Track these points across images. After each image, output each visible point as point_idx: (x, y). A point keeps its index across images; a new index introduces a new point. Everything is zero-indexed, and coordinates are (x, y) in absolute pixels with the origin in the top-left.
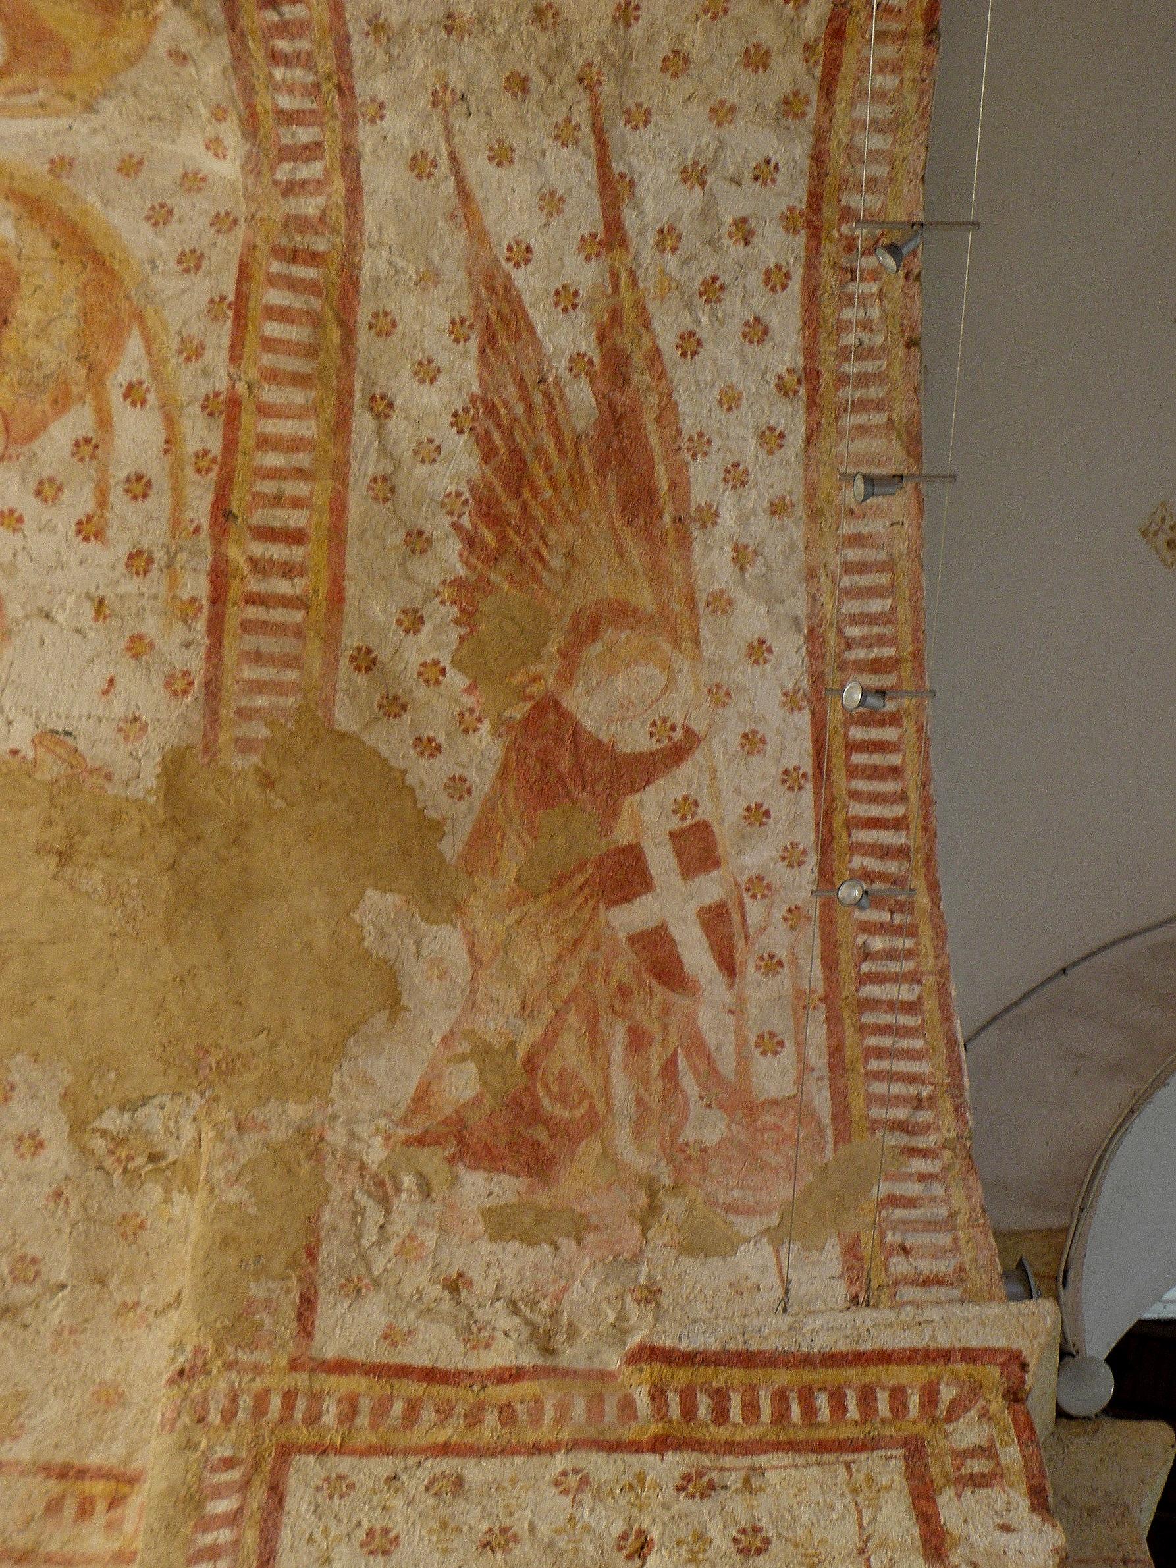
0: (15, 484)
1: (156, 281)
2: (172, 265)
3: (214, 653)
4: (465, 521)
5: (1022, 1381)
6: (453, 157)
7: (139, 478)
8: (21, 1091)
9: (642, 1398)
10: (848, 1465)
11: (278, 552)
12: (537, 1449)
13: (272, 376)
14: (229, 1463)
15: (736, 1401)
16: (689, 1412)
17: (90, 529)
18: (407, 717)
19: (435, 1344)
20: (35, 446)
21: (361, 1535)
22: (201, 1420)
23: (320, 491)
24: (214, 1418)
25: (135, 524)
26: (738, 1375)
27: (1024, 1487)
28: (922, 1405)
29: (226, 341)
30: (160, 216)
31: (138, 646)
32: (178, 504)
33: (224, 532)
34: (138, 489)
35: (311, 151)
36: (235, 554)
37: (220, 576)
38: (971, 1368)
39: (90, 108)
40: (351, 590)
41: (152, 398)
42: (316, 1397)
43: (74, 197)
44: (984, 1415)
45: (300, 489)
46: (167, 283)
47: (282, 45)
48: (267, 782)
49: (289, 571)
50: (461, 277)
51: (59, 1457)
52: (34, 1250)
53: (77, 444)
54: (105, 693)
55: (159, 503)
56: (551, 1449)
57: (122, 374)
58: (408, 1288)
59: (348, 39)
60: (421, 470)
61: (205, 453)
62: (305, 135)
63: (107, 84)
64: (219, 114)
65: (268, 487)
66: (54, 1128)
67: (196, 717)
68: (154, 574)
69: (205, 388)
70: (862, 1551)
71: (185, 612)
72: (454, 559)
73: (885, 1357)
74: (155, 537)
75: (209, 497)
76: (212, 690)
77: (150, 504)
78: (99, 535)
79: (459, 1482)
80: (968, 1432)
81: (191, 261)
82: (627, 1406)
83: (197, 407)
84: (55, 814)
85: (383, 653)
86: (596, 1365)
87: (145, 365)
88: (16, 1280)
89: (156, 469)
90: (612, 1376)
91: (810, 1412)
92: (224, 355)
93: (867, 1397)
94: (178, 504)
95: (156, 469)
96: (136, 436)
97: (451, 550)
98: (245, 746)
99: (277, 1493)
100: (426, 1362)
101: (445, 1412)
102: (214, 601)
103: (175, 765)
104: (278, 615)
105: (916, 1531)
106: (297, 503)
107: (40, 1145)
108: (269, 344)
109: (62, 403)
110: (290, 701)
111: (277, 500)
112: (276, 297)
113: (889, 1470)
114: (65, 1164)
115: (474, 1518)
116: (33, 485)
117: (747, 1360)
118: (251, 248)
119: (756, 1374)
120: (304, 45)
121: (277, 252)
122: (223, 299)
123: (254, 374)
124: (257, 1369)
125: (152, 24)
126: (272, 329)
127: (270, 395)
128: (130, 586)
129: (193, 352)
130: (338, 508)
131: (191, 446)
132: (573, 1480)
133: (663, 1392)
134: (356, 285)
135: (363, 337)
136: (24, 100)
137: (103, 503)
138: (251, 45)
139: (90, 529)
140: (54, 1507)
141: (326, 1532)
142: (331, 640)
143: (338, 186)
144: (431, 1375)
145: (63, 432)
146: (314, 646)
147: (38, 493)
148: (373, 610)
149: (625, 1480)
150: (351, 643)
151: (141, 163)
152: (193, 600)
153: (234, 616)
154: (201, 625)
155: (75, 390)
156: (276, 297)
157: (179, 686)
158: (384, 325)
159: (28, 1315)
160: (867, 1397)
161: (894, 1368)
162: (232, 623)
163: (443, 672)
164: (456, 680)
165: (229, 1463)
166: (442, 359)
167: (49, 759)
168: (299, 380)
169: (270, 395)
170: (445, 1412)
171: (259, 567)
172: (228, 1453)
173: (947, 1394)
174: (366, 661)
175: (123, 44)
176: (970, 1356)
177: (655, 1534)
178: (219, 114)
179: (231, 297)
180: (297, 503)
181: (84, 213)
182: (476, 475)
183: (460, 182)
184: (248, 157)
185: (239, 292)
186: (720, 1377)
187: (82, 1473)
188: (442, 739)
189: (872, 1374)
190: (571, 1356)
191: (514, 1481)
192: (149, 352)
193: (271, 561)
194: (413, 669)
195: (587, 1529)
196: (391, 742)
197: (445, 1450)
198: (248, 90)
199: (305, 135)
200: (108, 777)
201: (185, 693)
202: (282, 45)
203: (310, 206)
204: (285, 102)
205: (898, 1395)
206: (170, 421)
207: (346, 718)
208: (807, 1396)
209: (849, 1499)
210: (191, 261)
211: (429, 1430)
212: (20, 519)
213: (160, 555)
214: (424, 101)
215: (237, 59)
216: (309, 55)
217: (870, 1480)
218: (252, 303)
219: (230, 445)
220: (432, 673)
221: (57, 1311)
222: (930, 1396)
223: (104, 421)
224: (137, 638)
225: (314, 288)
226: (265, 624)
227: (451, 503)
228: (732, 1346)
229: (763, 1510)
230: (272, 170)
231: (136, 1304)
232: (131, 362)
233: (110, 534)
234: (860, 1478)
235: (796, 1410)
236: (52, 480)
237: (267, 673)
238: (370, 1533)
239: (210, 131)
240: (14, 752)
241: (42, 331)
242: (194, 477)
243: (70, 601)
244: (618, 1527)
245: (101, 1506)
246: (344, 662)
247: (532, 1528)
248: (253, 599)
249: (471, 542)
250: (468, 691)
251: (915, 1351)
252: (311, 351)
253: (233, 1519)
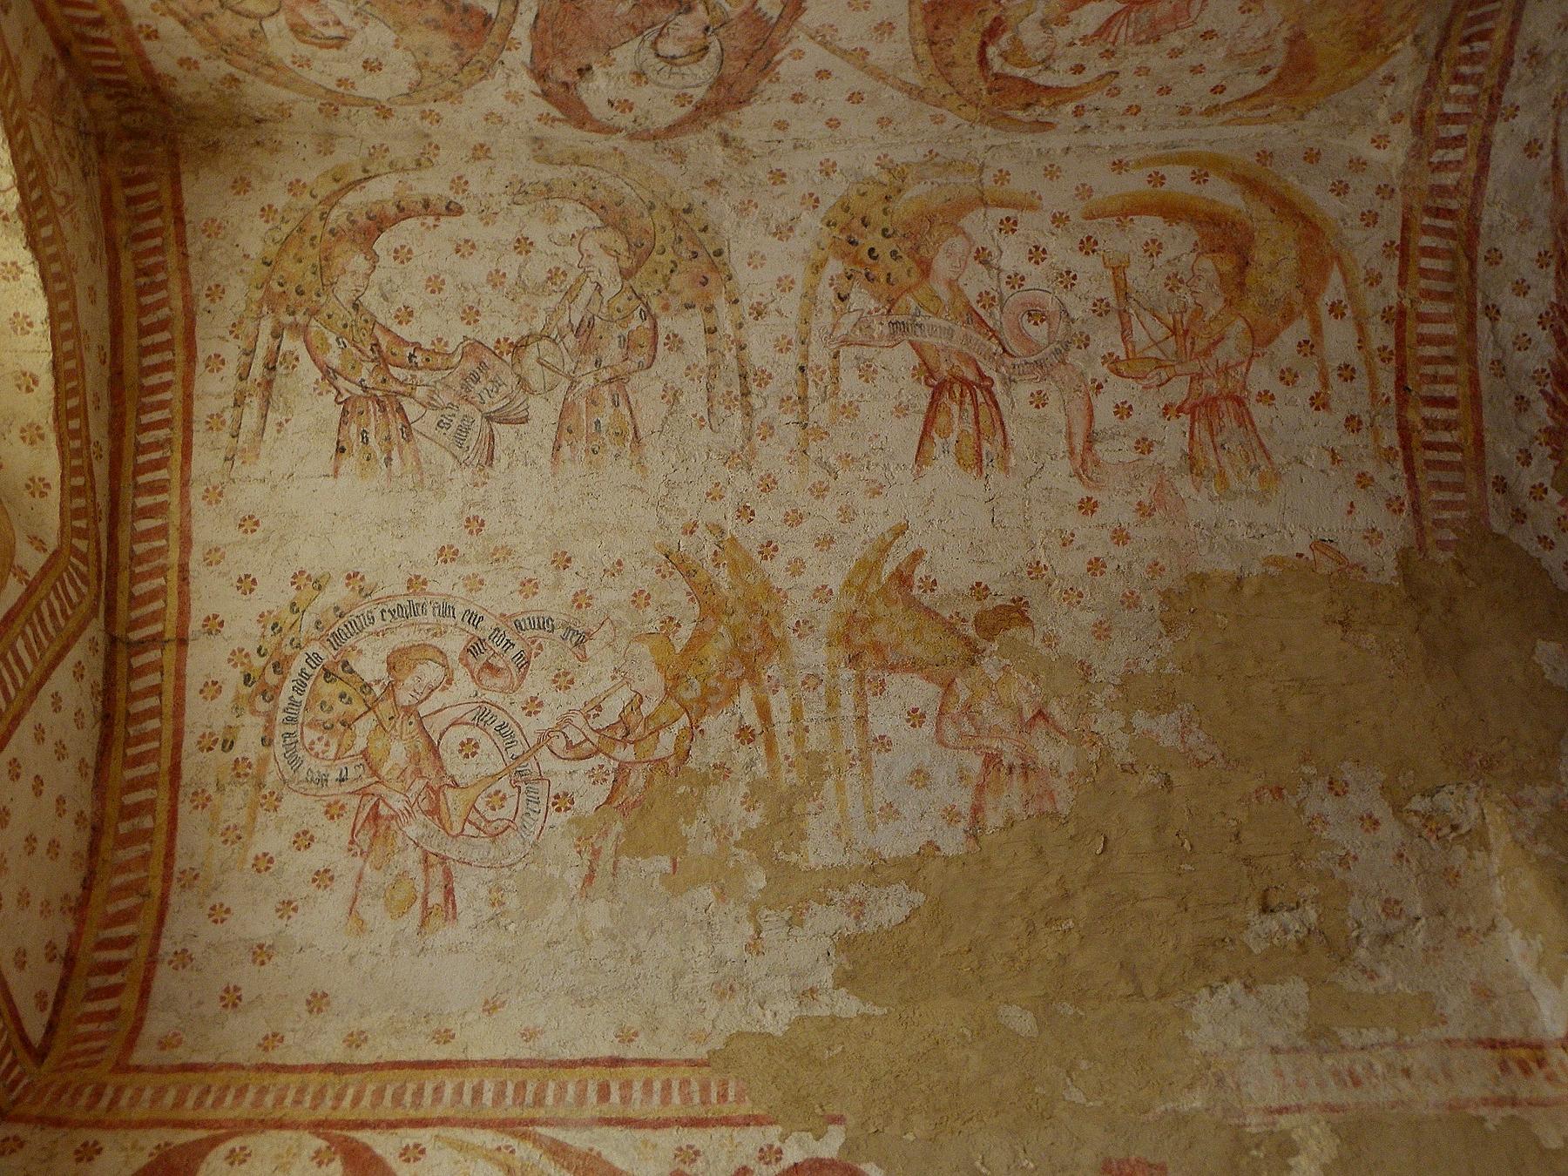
0: (1266, 373)
1: (1347, 233)
2: (1358, 222)
3: (1412, 483)
4: (1548, 388)
6: (1555, 142)
7: (1347, 366)
8: (1353, 787)
11: (1440, 413)
13: (1428, 294)
17: (1319, 403)
18: (1529, 522)
20: (1272, 347)
23: (1460, 371)
25: (1348, 398)
29: (1396, 271)
30: (1341, 189)
31: (1363, 480)
32: (1374, 384)
33: (1406, 401)
34: (1346, 373)
35: (1459, 141)
36: (1413, 416)
37: (1405, 431)
39: (1302, 117)
40: (1488, 438)
41: (1348, 312)
43: (1278, 178)
45: (1447, 370)
46: (1354, 233)
47: (1465, 69)
48: (1461, 570)
49: (1448, 426)
50: (1546, 223)
51: (1483, 1033)
52: (1395, 895)
53: (1300, 345)
54: (1350, 512)
55: (1362, 382)
57: (1327, 298)
59: (1512, 63)
60: (1519, 355)
61: (1385, 348)
62: (1455, 130)
63: (1321, 100)
64: (1396, 118)
65: (1429, 370)
66: (1381, 810)
67: (1411, 527)
68: (1364, 431)
69: (1383, 304)
71: (1388, 456)
72: (1545, 415)
74: (1362, 407)
75: (1393, 378)
76: (1416, 510)
77: (1355, 384)
78: (1325, 406)
81: (1370, 219)
83: (1378, 317)
84: (1335, 596)
85: (1510, 480)
87: (1343, 290)
89: (1356, 360)
92: (1395, 281)
94: (1374, 384)
95: (1356, 360)
96: (1339, 339)
97: (1542, 407)
98: (1443, 545)
102: (1404, 448)
103: (1404, 558)
104: (1445, 456)
106: (1448, 380)
107: (1376, 823)
108: (1424, 273)
109: (1288, 317)
110: (1463, 514)
111: (1434, 379)
112: (1427, 241)
114: (1398, 835)
116: (1278, 374)
118: (1409, 209)
120: (1479, 69)
121: (1428, 211)
122: (1393, 243)
123: (1415, 293)
125: (1386, 57)
126: (1426, 263)
127: (1426, 307)
128: (1350, 439)
129: (1374, 280)
130: (1474, 382)
131: (1375, 344)
134: (1477, 232)
135: (1481, 266)
136: (1260, 112)
137: (1325, 385)
138: (1444, 69)
139: (1319, 403)
142: (1481, 471)
143: (1473, 164)
145: (1290, 338)
146: (1472, 476)
147: (1282, 379)
148: (1502, 450)
150: (1492, 474)
151: (1318, 153)
152: (1391, 448)
153: (1420, 457)
154: (1399, 465)
155: (1297, 308)
156: (1427, 241)
157: (1396, 506)
158: (1495, 257)
159: (1401, 938)
162: (1419, 462)
163: (1546, 491)
164: (1554, 496)
166: (1531, 280)
167: (1324, 559)
168: (1445, 296)
169: (1426, 307)
171: (1430, 424)
174: (1501, 485)
175: (1355, 71)
178: (1396, 118)
179: (1398, 242)
180: (1448, 380)
181: (1287, 188)
182: (1553, 358)
183: (1556, 158)
184: (1414, 146)
185: (1403, 238)
187: (1503, 1044)
188: (1552, 536)
192: (1345, 280)
193: (1436, 420)
194: (1527, 489)
196: (1524, 538)
198: (1427, 99)
199: (1455, 130)
200: (1364, 569)
201: (1401, 511)
202: (1465, 69)
203: (1449, 179)
204: (1449, 108)
206: (1361, 328)
207: (1498, 525)
210: (1370, 219)
212: (1272, 397)
213: (1365, 418)
214: (1547, 105)
215: (1429, 79)
216: (1481, 75)
218: (1412, 245)
219: (1400, 342)
220: (1538, 492)
221: (1419, 937)
223: (1317, 329)
224: (1362, 475)
225: (1451, 234)
226: (1440, 462)
227: (1537, 377)
230: (1430, 155)
231: (1469, 929)
232: (1334, 288)
233: (1333, 405)
236: (1289, 370)
237: (1446, 496)
239: (1382, 130)
240: (1300, 555)
241: (1273, 269)
242: (1380, 364)
243: (1314, 451)
245: (1533, 1065)
246: (1490, 486)
248: (1429, 446)
249: (1554, 402)
250: (1561, 503)
252: (1451, 277)
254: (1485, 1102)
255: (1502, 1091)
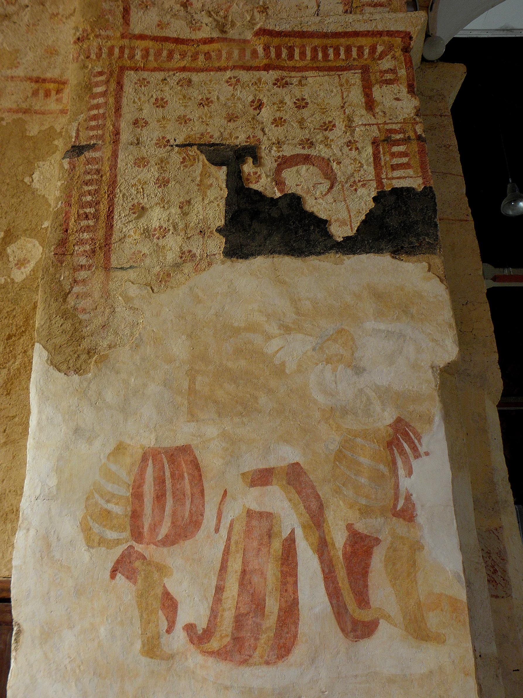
5: (410, 44)
9: (260, 50)
10: (339, 76)
12: (219, 69)
14: (101, 74)
15: (297, 51)
16: (278, 55)
19: (178, 28)
21: (153, 100)
22: (88, 57)
24: (93, 56)
26: (298, 41)
27: (406, 84)
28: (369, 53)
38: (390, 39)
42: (132, 49)
44: (394, 57)
51: (35, 75)
56: (225, 69)
58: (167, 6)
70: (343, 107)
73: (356, 34)
79: (190, 81)
80: (386, 64)
82: (254, 53)
86: (242, 37)
88: (8, 3)
90: (249, 41)
91: (326, 55)
93: (348, 50)
99: (120, 85)
100: (175, 35)
101: (183, 55)
105: (363, 100)
113: (355, 78)
115: (196, 94)
117: (302, 35)
119: (305, 41)
124: (108, 37)
132: (233, 81)
133: (269, 47)
140: (35, 93)
141: (139, 99)
144: (177, 41)
149: (253, 81)
159: (15, 18)
160: (348, 50)
161: (360, 39)
165: (101, 74)
170: (183, 55)
172: (100, 70)
173: (380, 49)
176: (390, 34)
177: (265, 101)
186: (291, 42)
187: (44, 81)
189: (350, 41)
190: (232, 33)
191: (211, 81)
195: (239, 99)
197: (184, 69)
205: (360, 49)
208: (325, 50)
209: (339, 88)
211: (177, 61)
217: (347, 81)
221: (26, 16)
222: (373, 49)
228: (296, 29)
229: (306, 93)
231: (58, 14)
234: (343, 81)
235: (320, 55)
238: (157, 99)
244: (251, 98)
245: (53, 93)
247: (218, 98)
251: (369, 32)
253: (104, 94)
254: (10, 110)
255: (24, 106)
